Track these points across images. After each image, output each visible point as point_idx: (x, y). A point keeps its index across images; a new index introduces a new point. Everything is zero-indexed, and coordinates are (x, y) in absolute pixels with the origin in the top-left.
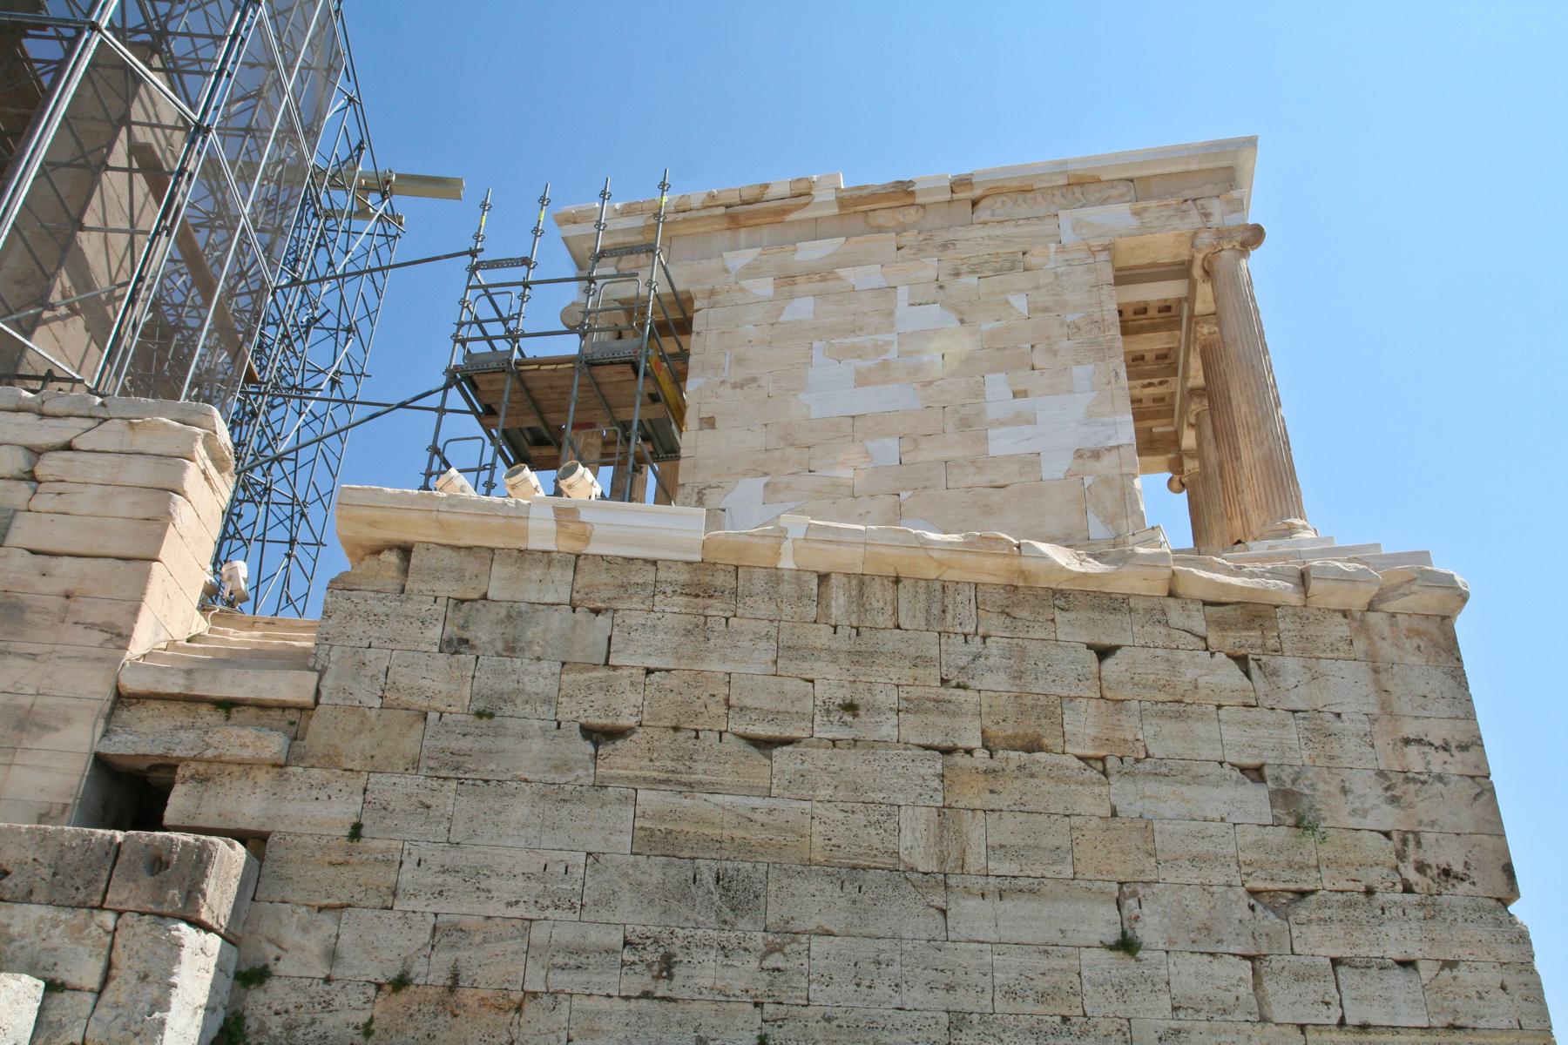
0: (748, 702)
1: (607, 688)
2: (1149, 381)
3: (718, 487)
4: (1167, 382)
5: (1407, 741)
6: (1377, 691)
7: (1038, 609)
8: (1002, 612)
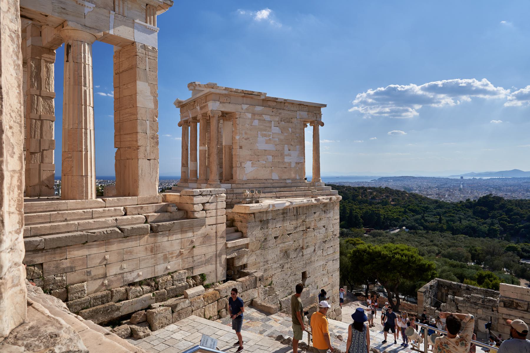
0: (288, 229)
1: (276, 231)
5: (335, 219)
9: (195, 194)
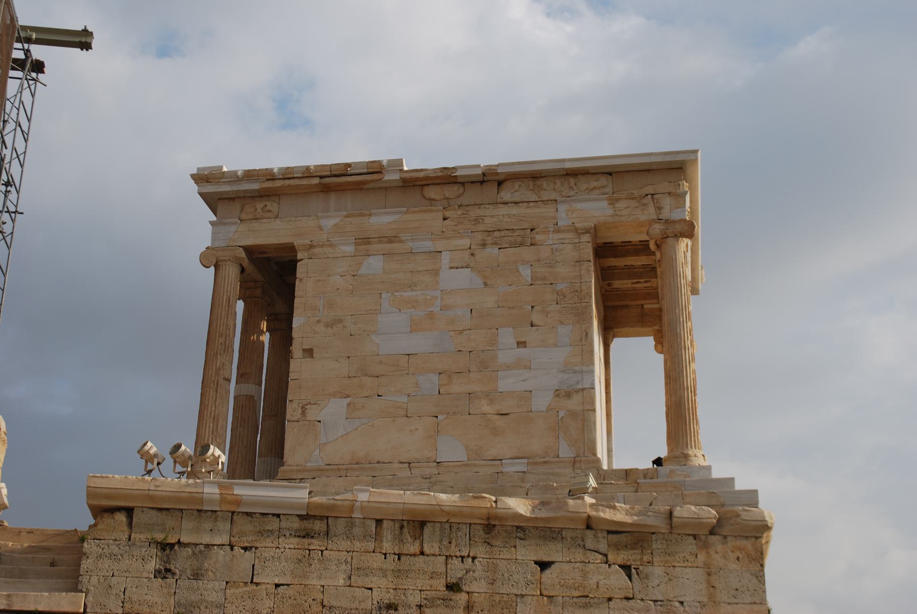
0: (334, 603)
1: (252, 596)
2: (637, 280)
3: (316, 404)
4: (650, 281)
6: (707, 587)
7: (506, 539)
8: (485, 542)
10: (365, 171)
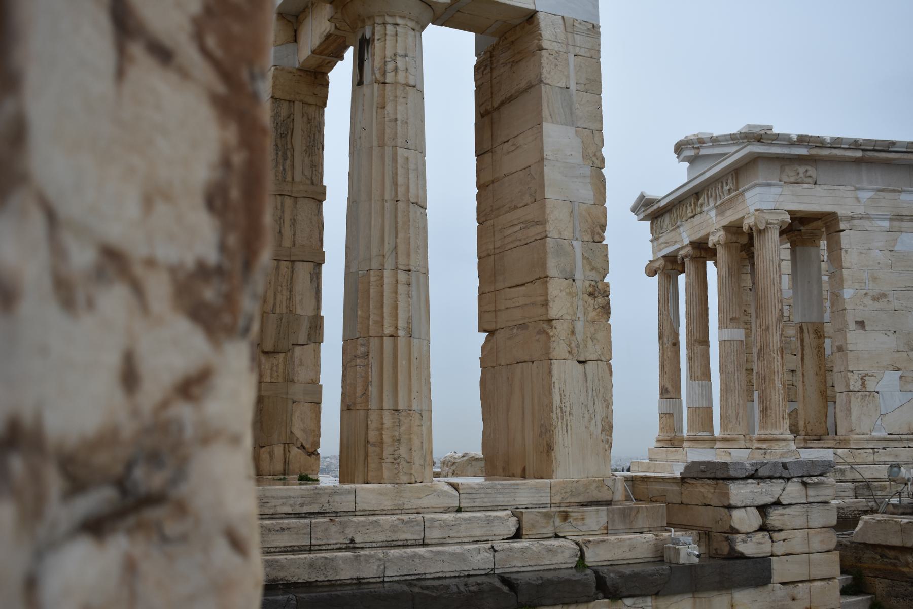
9: (733, 473)
10: (905, 150)
